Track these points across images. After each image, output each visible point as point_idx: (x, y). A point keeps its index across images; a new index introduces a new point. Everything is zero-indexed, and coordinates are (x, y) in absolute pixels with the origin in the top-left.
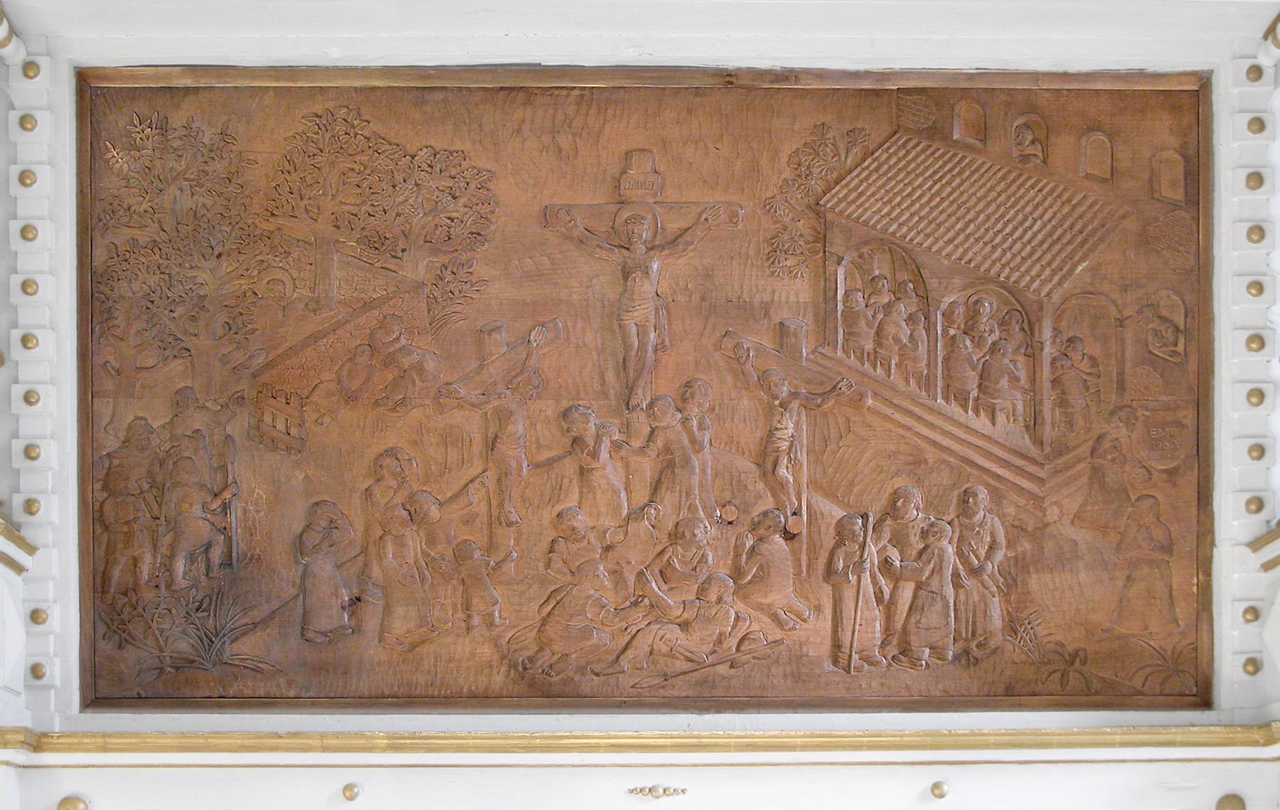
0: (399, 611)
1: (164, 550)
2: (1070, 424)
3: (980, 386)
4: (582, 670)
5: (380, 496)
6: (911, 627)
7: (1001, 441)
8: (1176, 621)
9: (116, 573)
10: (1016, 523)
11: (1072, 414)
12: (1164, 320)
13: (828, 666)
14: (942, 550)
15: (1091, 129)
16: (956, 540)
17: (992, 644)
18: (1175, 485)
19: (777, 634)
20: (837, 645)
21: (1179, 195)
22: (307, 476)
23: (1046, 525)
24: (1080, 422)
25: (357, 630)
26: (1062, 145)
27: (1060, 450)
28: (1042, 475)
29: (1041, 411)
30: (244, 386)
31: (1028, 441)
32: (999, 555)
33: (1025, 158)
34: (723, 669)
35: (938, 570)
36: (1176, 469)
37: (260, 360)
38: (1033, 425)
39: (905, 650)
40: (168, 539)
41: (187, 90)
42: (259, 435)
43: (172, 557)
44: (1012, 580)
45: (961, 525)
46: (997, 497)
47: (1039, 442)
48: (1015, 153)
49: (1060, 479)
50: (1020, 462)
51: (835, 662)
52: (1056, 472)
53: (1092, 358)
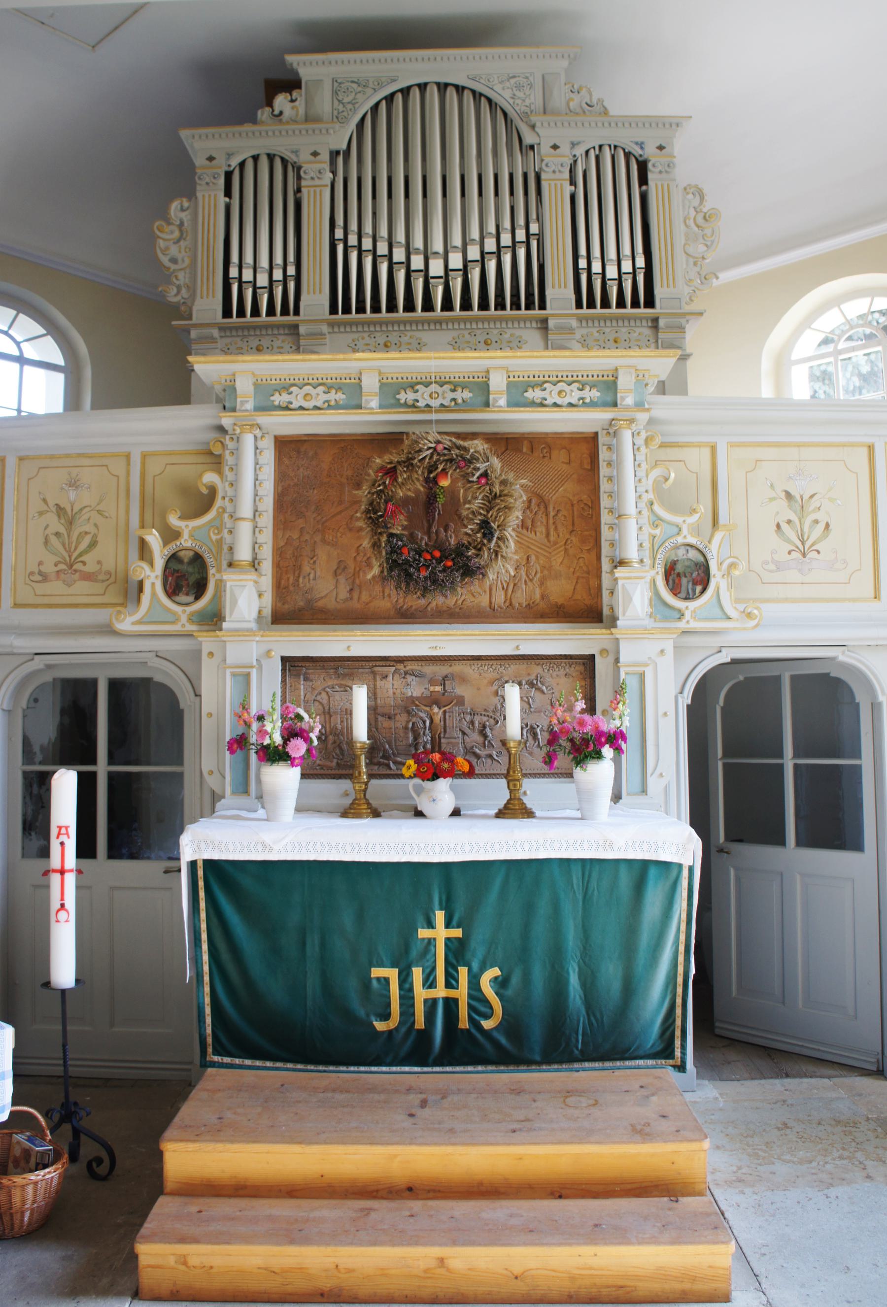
0: (364, 593)
1: (296, 575)
2: (559, 536)
4: (416, 610)
5: (359, 558)
6: (512, 597)
8: (591, 595)
9: (283, 582)
12: (586, 504)
13: (488, 609)
15: (563, 448)
17: (537, 602)
19: (473, 599)
20: (491, 603)
21: (589, 467)
22: (338, 554)
24: (561, 535)
25: (351, 598)
26: (555, 453)
27: (556, 543)
30: (320, 526)
31: (546, 540)
32: (538, 575)
33: (544, 457)
34: (457, 610)
35: (520, 580)
36: (590, 549)
37: (324, 519)
38: (548, 535)
39: (511, 604)
40: (297, 573)
41: (305, 441)
42: (324, 541)
43: (299, 577)
44: (542, 583)
46: (537, 558)
47: (549, 541)
48: (541, 455)
49: (556, 552)
50: (544, 547)
51: (490, 608)
52: (554, 550)
53: (564, 516)
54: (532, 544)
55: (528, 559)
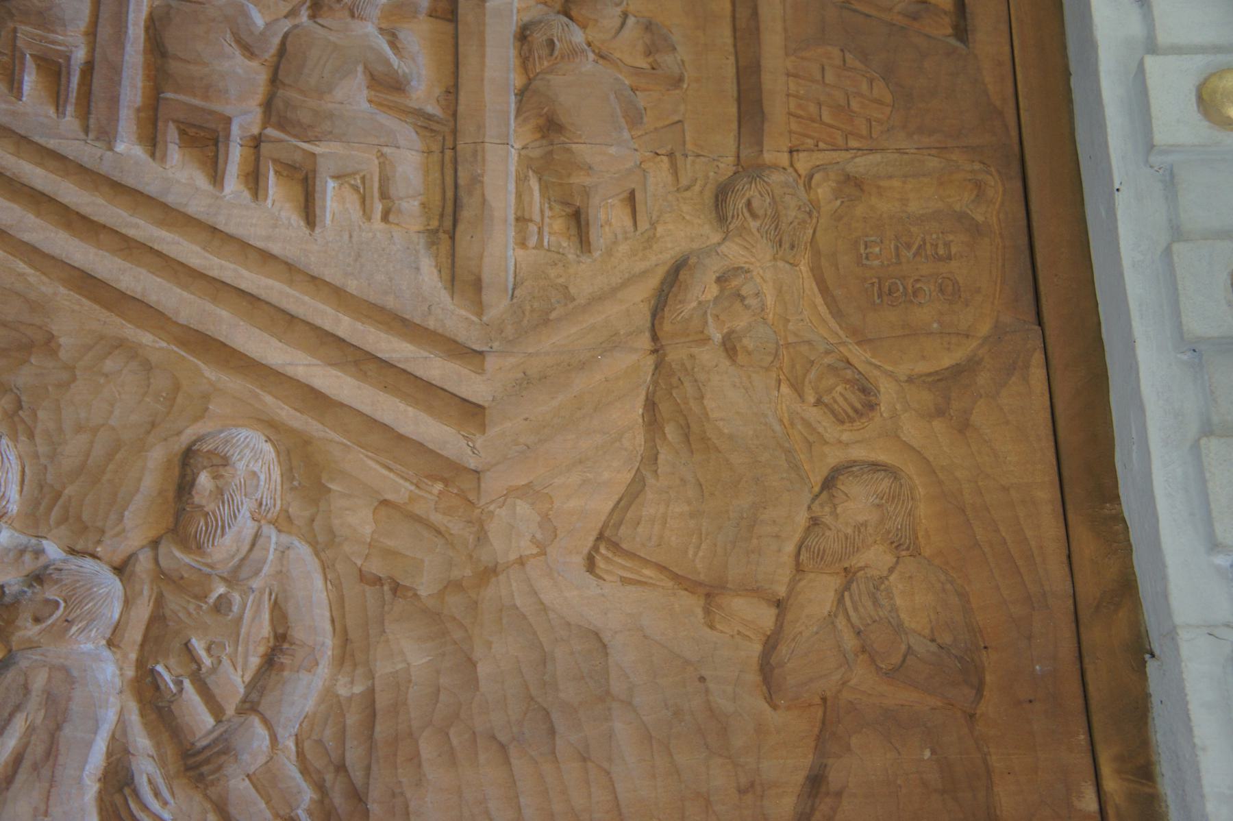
2: (578, 221)
3: (268, 105)
7: (331, 274)
10: (376, 567)
11: (586, 192)
14: (66, 675)
16: (135, 634)
18: (964, 427)
23: (489, 573)
28: (474, 387)
29: (476, 180)
31: (429, 276)
36: (957, 371)
45: (161, 575)
54: (250, 301)
55: (184, 487)
